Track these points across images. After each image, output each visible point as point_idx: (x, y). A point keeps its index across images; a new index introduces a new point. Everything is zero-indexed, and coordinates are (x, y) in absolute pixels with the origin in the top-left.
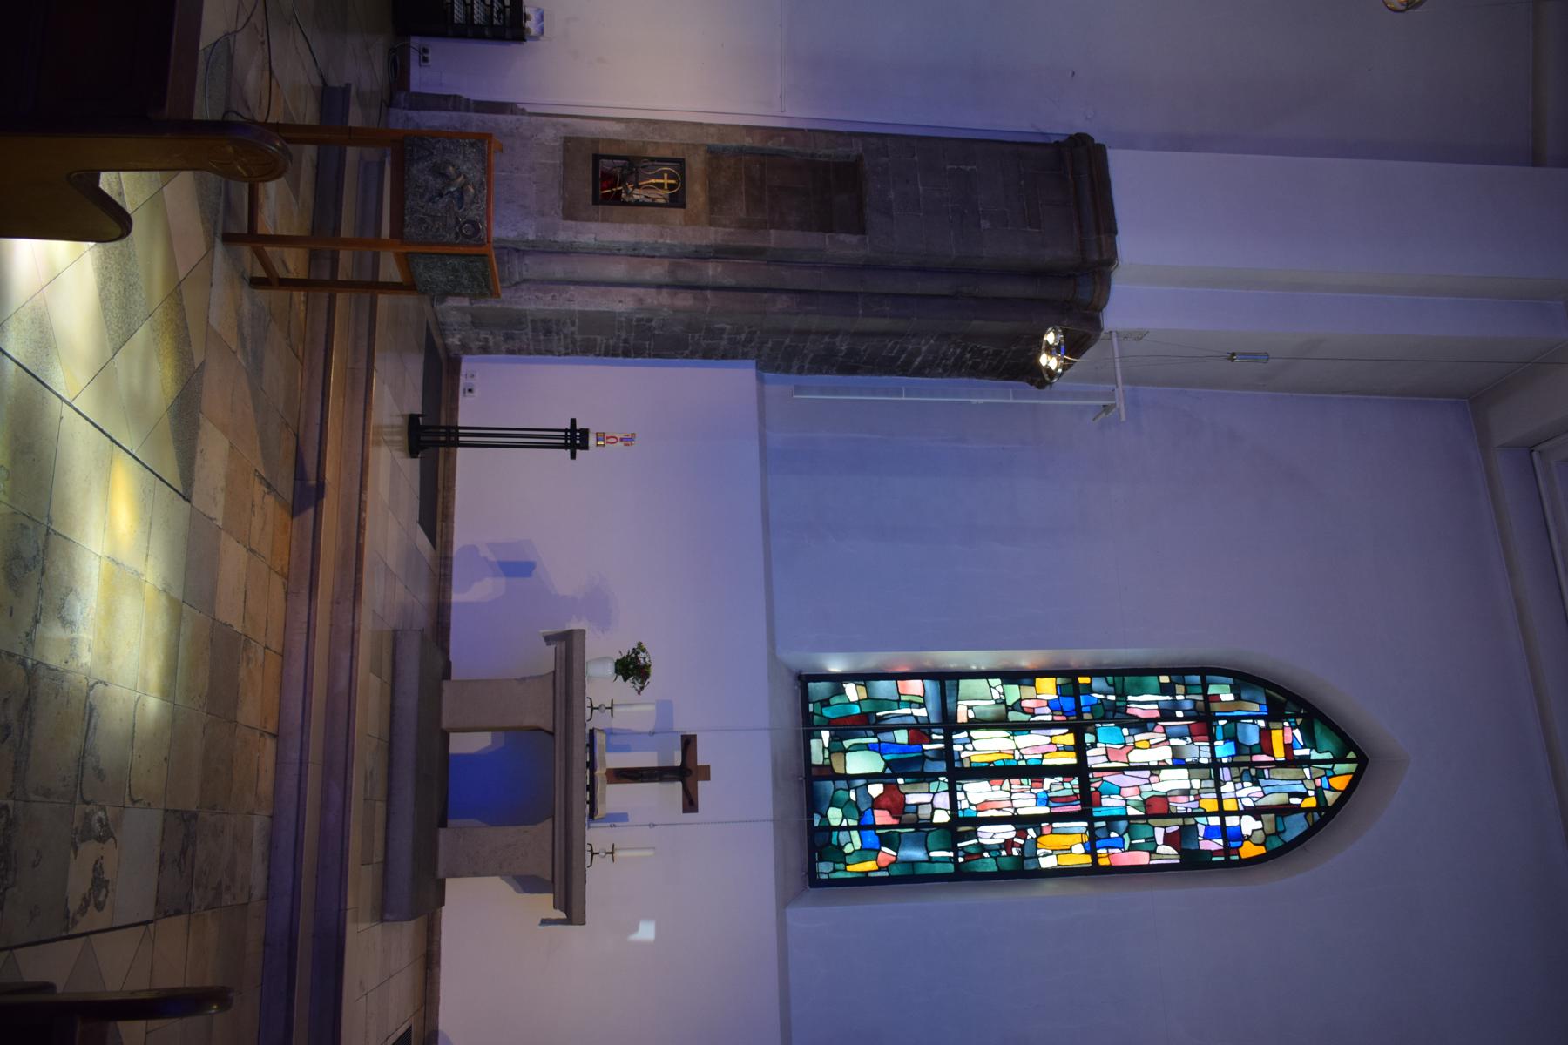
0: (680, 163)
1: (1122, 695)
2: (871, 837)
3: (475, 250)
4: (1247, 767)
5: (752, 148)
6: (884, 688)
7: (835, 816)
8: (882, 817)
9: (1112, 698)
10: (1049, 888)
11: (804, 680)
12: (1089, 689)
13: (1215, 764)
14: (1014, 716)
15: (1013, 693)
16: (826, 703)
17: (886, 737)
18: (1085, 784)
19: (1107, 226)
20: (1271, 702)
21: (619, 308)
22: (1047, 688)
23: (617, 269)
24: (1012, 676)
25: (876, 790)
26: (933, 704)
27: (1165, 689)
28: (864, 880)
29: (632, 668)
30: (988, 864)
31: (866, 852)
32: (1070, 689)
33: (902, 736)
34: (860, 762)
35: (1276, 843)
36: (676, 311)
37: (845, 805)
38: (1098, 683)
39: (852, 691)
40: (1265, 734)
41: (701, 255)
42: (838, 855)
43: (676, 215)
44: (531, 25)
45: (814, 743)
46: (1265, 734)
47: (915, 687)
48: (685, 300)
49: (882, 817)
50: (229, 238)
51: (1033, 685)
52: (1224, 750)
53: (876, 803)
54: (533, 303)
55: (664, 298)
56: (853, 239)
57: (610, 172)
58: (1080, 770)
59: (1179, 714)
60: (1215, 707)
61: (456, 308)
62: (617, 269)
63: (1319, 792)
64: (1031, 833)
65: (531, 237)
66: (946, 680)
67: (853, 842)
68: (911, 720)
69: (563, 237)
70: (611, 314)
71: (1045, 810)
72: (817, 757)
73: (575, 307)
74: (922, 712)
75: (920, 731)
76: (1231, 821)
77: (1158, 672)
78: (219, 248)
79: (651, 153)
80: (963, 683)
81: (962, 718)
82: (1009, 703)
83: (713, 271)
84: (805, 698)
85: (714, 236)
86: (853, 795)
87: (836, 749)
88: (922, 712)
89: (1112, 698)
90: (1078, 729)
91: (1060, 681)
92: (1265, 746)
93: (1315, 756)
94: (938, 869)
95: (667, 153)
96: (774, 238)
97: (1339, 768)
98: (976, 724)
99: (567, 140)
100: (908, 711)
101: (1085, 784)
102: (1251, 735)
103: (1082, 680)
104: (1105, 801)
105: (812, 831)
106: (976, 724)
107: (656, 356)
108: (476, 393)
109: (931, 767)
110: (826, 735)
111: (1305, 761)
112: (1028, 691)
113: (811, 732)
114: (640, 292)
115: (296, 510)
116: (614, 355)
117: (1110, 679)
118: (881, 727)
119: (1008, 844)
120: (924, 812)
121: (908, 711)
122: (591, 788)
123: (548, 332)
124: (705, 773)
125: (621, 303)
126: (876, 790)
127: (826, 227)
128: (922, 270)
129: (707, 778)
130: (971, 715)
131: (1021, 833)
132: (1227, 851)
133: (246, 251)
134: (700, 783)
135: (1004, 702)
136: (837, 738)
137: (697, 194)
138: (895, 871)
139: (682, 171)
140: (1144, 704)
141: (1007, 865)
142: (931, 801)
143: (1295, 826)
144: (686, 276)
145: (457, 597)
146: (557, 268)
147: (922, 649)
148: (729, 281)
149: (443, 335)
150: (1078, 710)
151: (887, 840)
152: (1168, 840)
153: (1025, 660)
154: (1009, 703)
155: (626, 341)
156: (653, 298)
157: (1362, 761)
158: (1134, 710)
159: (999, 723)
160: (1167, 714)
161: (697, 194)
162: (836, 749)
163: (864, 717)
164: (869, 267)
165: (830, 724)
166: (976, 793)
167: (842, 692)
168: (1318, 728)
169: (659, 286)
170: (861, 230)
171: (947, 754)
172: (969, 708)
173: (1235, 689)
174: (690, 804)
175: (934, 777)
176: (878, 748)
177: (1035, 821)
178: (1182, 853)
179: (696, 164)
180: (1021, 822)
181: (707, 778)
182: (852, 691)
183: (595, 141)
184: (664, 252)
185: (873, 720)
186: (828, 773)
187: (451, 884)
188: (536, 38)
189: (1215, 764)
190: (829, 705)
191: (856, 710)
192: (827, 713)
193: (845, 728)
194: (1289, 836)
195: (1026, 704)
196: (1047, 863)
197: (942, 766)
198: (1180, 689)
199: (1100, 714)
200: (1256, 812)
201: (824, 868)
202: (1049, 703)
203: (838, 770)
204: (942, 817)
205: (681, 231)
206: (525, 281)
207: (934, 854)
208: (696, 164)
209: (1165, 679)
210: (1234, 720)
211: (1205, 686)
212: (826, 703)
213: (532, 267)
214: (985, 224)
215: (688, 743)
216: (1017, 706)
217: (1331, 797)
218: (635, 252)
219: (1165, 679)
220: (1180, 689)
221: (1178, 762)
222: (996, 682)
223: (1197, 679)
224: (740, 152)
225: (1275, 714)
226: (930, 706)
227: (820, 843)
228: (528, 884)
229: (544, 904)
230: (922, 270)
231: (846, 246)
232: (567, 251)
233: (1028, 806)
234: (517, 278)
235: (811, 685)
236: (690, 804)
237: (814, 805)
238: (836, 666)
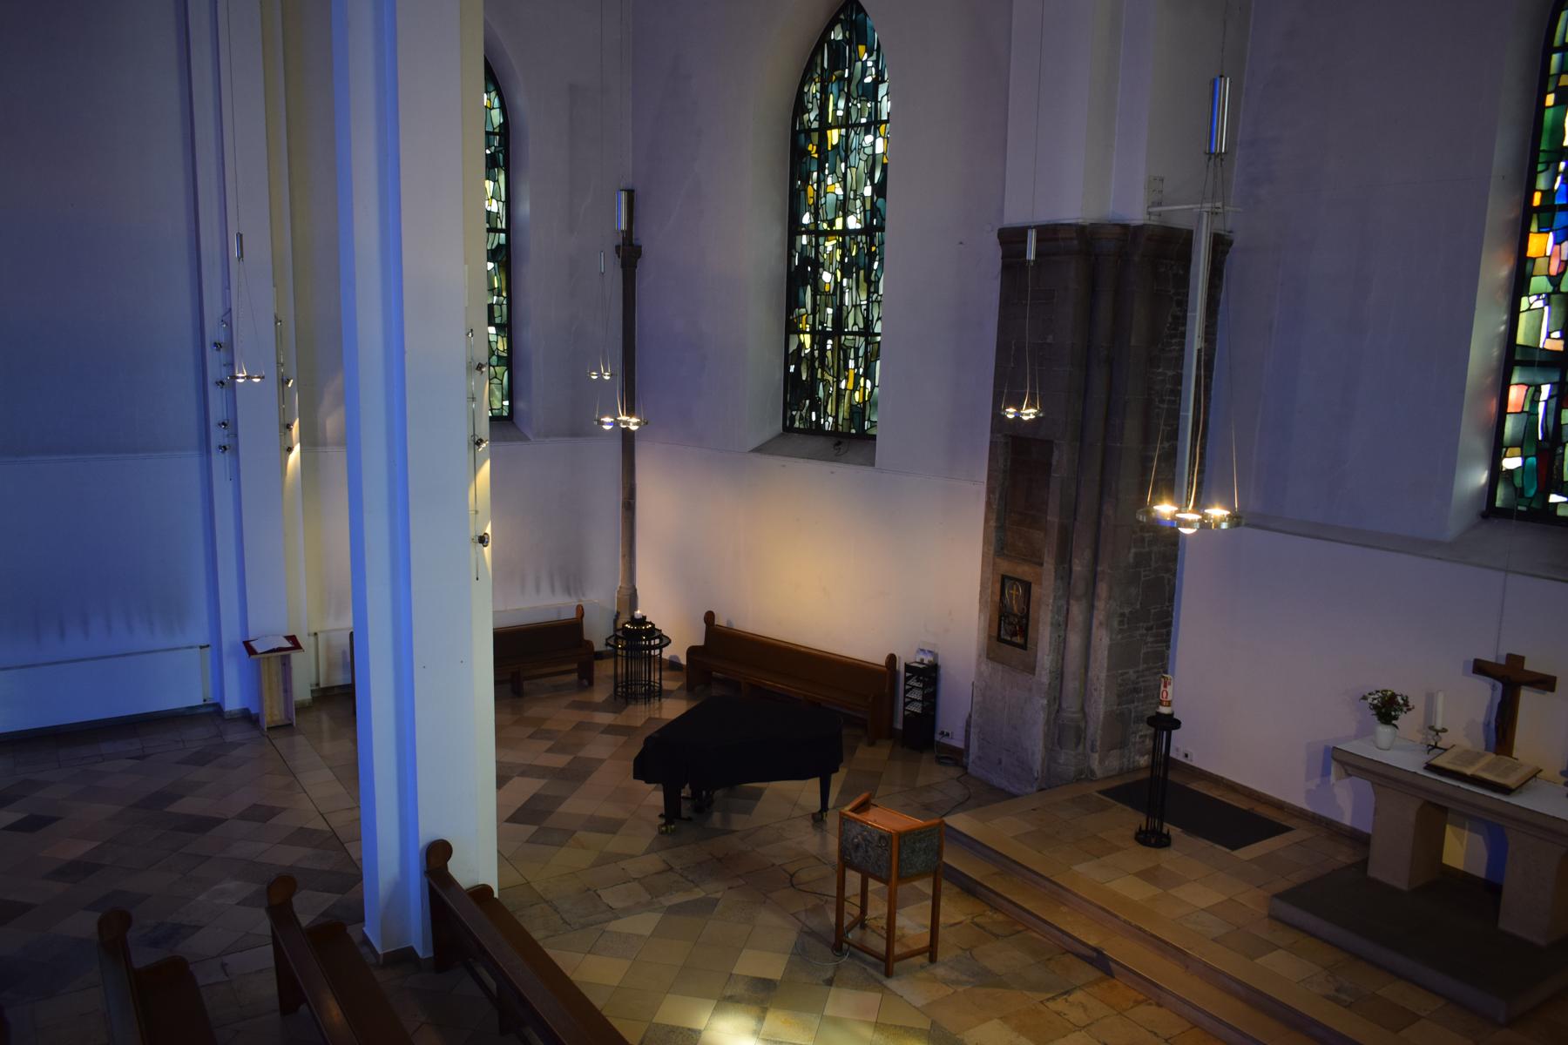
0: (1004, 578)
3: (895, 844)
5: (998, 519)
9: (1562, 165)
11: (1489, 512)
12: (1548, 194)
15: (1539, 283)
16: (1519, 492)
21: (1106, 641)
22: (1540, 244)
23: (1075, 641)
24: (1520, 285)
32: (1545, 216)
36: (1110, 598)
38: (1542, 183)
39: (1511, 463)
43: (1035, 589)
44: (927, 659)
45: (1560, 512)
47: (1516, 394)
48: (1103, 589)
50: (888, 974)
51: (1534, 259)
54: (1100, 707)
55: (1100, 605)
56: (1056, 453)
57: (1009, 627)
61: (1101, 761)
62: (1075, 641)
65: (1045, 702)
66: (1514, 357)
68: (1553, 403)
69: (1045, 679)
70: (1110, 648)
73: (1103, 675)
74: (1546, 390)
77: (1541, 107)
78: (892, 984)
79: (997, 598)
80: (1520, 340)
82: (1550, 289)
84: (1506, 513)
85: (1049, 565)
88: (1546, 390)
89: (1562, 165)
91: (1534, 227)
95: (998, 586)
100: (1541, 407)
103: (1537, 199)
107: (1171, 599)
108: (1189, 750)
110: (1554, 498)
112: (1540, 264)
114: (1095, 623)
115: (1109, 973)
116: (1169, 634)
117: (1540, 167)
121: (1541, 407)
123: (1136, 690)
125: (1102, 640)
129: (1522, 659)
130: (1557, 335)
133: (897, 966)
134: (1527, 667)
135: (1548, 295)
137: (1023, 571)
139: (1011, 578)
144: (1080, 587)
145: (1347, 820)
146: (1071, 685)
147: (1463, 392)
148: (1088, 554)
149: (1138, 769)
153: (1496, 270)
154: (1550, 289)
155: (1148, 629)
156: (1099, 616)
161: (1023, 571)
169: (1092, 607)
172: (1548, 336)
174: (1546, 683)
179: (1005, 567)
181: (1522, 659)
182: (1511, 463)
183: (990, 637)
184: (1062, 602)
185: (1547, 445)
188: (936, 656)
190: (1522, 489)
191: (1532, 460)
192: (1532, 492)
195: (1554, 270)
202: (1557, 242)
205: (1046, 591)
206: (1083, 709)
208: (1005, 567)
212: (1519, 492)
213: (1071, 704)
214: (1050, 339)
215: (1480, 668)
218: (1062, 625)
219: (1550, 100)
224: (1001, 528)
226: (1539, 380)
232: (1059, 675)
234: (1078, 716)
235: (1498, 504)
236: (1546, 683)
238: (1482, 477)
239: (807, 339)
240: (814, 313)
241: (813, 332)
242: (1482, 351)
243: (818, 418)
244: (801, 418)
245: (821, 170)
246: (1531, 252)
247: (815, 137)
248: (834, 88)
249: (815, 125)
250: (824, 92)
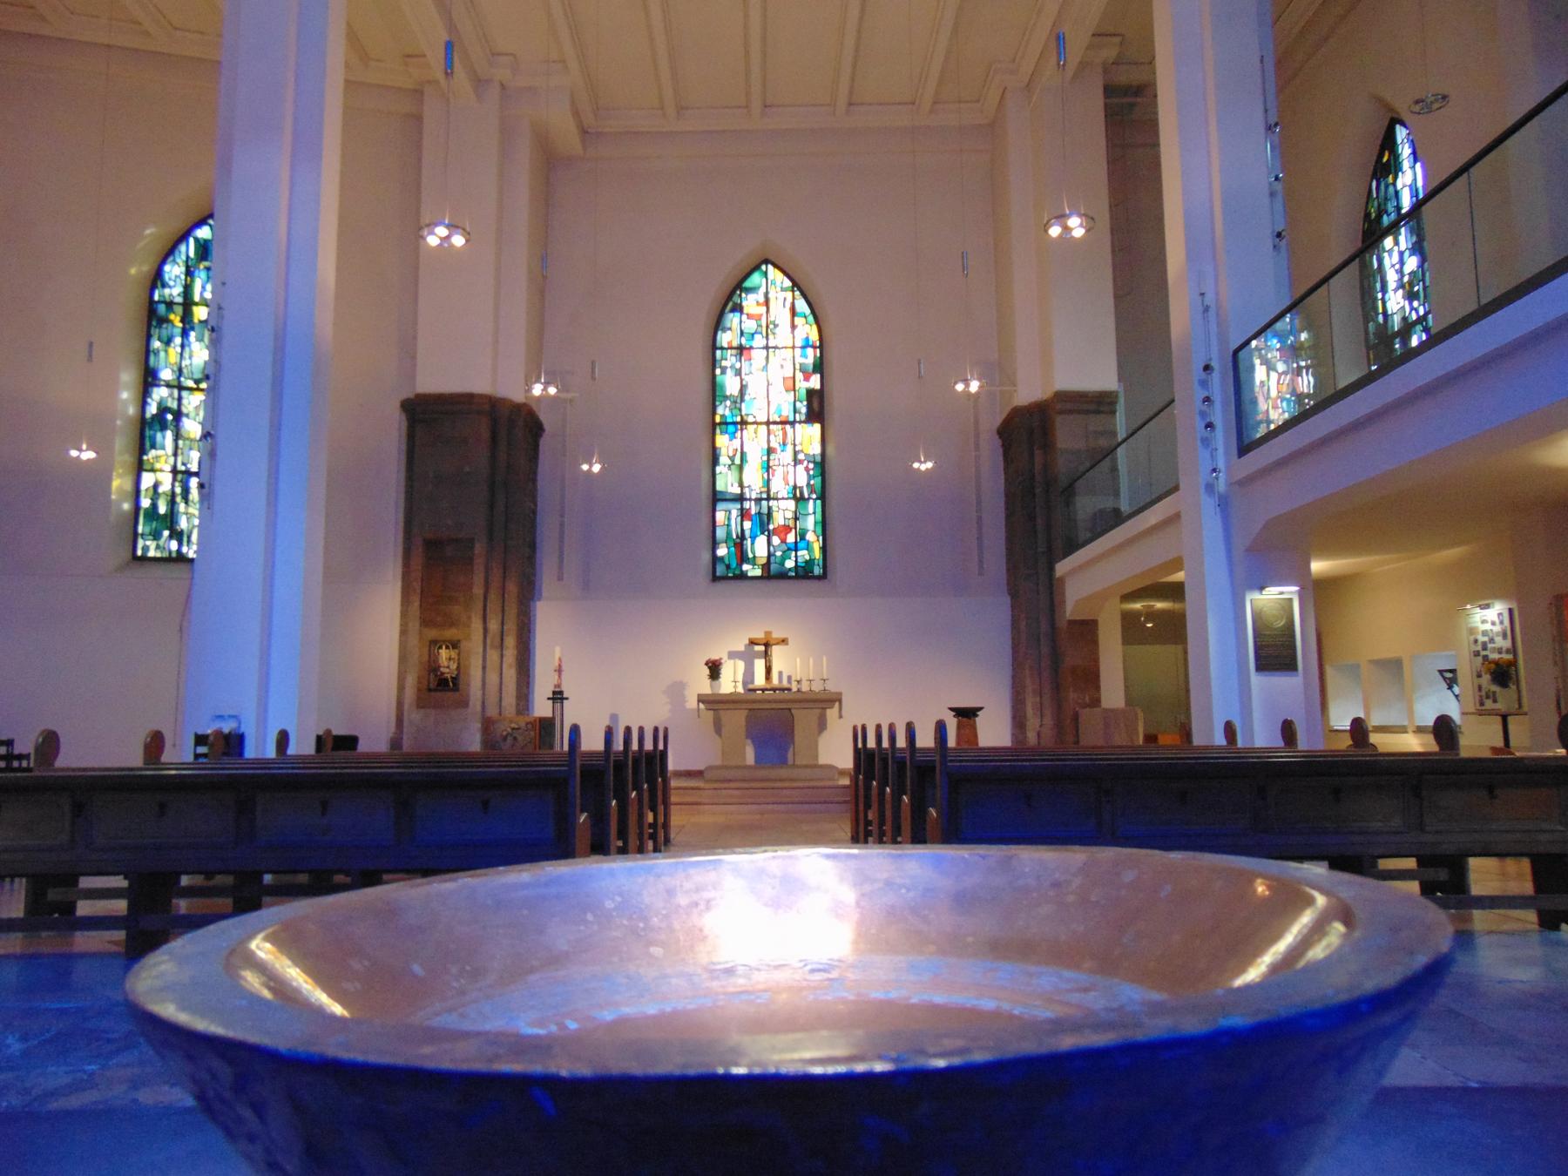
1: (726, 398)
2: (801, 545)
4: (770, 328)
6: (721, 533)
7: (790, 564)
8: (791, 538)
10: (830, 450)
13: (767, 348)
14: (738, 461)
15: (724, 460)
16: (728, 567)
17: (747, 533)
18: (775, 423)
19: (469, 398)
20: (733, 310)
23: (493, 678)
24: (715, 460)
25: (776, 540)
26: (730, 506)
27: (724, 371)
28: (824, 549)
29: (714, 669)
30: (817, 482)
31: (808, 547)
33: (747, 525)
34: (760, 548)
35: (811, 318)
37: (783, 558)
38: (720, 410)
39: (722, 551)
40: (749, 316)
41: (485, 630)
42: (810, 563)
43: (463, 645)
46: (749, 316)
47: (720, 516)
49: (791, 538)
52: (759, 341)
53: (783, 541)
58: (768, 423)
59: (738, 365)
60: (735, 344)
62: (493, 678)
63: (783, 290)
64: (801, 456)
67: (803, 555)
71: (790, 448)
72: (758, 572)
75: (744, 514)
76: (799, 343)
77: (714, 376)
79: (426, 658)
80: (720, 486)
81: (738, 491)
83: (494, 626)
85: (477, 624)
86: (779, 554)
87: (753, 562)
88: (735, 513)
90: (744, 423)
92: (758, 318)
93: (763, 289)
94: (819, 510)
96: (478, 591)
97: (770, 276)
98: (741, 485)
99: (419, 707)
101: (775, 423)
102: (750, 325)
104: (785, 413)
105: (797, 577)
106: (741, 485)
109: (765, 511)
110: (745, 567)
111: (766, 295)
112: (723, 451)
113: (743, 576)
118: (742, 537)
119: (807, 469)
120: (790, 515)
122: (774, 690)
124: (768, 633)
126: (776, 540)
127: (471, 560)
128: (492, 506)
131: (801, 462)
132: (814, 347)
136: (747, 561)
137: (450, 633)
138: (819, 531)
140: (730, 384)
141: (819, 471)
142: (783, 512)
143: (802, 306)
150: (735, 423)
151: (803, 538)
152: (807, 379)
157: (766, 262)
158: (736, 392)
159: (741, 468)
160: (738, 373)
161: (450, 633)
162: (753, 562)
163: (735, 545)
164: (491, 538)
165: (740, 564)
166: (779, 486)
167: (722, 559)
168: (747, 284)
170: (472, 540)
171: (758, 500)
173: (724, 330)
175: (769, 508)
176: (753, 538)
177: (796, 453)
178: (814, 371)
179: (433, 633)
180: (796, 462)
182: (722, 551)
183: (419, 690)
186: (766, 566)
187: (822, 761)
189: (767, 348)
193: (742, 557)
194: (808, 311)
196: (817, 450)
197: (764, 503)
198: (724, 363)
199: (736, 412)
200: (793, 327)
201: (817, 571)
203: (764, 561)
204: (791, 504)
205: (474, 643)
207: (811, 510)
209: (718, 371)
210: (742, 333)
211: (722, 348)
212: (728, 567)
214: (467, 469)
215: (753, 642)
216: (732, 459)
217: (788, 283)
220: (724, 363)
221: (765, 368)
222: (718, 469)
223: (718, 353)
225: (738, 308)
227: (804, 573)
228: (822, 725)
229: (832, 713)
230: (492, 506)
231: (479, 548)
233: (787, 456)
236: (784, 641)
237: (783, 575)
239: (166, 481)
240: (175, 455)
241: (175, 471)
242: (705, 492)
243: (180, 544)
244: (158, 547)
245: (185, 334)
246: (718, 444)
247: (179, 309)
248: (203, 275)
249: (179, 300)
250: (189, 273)
